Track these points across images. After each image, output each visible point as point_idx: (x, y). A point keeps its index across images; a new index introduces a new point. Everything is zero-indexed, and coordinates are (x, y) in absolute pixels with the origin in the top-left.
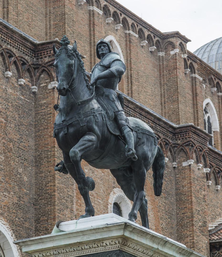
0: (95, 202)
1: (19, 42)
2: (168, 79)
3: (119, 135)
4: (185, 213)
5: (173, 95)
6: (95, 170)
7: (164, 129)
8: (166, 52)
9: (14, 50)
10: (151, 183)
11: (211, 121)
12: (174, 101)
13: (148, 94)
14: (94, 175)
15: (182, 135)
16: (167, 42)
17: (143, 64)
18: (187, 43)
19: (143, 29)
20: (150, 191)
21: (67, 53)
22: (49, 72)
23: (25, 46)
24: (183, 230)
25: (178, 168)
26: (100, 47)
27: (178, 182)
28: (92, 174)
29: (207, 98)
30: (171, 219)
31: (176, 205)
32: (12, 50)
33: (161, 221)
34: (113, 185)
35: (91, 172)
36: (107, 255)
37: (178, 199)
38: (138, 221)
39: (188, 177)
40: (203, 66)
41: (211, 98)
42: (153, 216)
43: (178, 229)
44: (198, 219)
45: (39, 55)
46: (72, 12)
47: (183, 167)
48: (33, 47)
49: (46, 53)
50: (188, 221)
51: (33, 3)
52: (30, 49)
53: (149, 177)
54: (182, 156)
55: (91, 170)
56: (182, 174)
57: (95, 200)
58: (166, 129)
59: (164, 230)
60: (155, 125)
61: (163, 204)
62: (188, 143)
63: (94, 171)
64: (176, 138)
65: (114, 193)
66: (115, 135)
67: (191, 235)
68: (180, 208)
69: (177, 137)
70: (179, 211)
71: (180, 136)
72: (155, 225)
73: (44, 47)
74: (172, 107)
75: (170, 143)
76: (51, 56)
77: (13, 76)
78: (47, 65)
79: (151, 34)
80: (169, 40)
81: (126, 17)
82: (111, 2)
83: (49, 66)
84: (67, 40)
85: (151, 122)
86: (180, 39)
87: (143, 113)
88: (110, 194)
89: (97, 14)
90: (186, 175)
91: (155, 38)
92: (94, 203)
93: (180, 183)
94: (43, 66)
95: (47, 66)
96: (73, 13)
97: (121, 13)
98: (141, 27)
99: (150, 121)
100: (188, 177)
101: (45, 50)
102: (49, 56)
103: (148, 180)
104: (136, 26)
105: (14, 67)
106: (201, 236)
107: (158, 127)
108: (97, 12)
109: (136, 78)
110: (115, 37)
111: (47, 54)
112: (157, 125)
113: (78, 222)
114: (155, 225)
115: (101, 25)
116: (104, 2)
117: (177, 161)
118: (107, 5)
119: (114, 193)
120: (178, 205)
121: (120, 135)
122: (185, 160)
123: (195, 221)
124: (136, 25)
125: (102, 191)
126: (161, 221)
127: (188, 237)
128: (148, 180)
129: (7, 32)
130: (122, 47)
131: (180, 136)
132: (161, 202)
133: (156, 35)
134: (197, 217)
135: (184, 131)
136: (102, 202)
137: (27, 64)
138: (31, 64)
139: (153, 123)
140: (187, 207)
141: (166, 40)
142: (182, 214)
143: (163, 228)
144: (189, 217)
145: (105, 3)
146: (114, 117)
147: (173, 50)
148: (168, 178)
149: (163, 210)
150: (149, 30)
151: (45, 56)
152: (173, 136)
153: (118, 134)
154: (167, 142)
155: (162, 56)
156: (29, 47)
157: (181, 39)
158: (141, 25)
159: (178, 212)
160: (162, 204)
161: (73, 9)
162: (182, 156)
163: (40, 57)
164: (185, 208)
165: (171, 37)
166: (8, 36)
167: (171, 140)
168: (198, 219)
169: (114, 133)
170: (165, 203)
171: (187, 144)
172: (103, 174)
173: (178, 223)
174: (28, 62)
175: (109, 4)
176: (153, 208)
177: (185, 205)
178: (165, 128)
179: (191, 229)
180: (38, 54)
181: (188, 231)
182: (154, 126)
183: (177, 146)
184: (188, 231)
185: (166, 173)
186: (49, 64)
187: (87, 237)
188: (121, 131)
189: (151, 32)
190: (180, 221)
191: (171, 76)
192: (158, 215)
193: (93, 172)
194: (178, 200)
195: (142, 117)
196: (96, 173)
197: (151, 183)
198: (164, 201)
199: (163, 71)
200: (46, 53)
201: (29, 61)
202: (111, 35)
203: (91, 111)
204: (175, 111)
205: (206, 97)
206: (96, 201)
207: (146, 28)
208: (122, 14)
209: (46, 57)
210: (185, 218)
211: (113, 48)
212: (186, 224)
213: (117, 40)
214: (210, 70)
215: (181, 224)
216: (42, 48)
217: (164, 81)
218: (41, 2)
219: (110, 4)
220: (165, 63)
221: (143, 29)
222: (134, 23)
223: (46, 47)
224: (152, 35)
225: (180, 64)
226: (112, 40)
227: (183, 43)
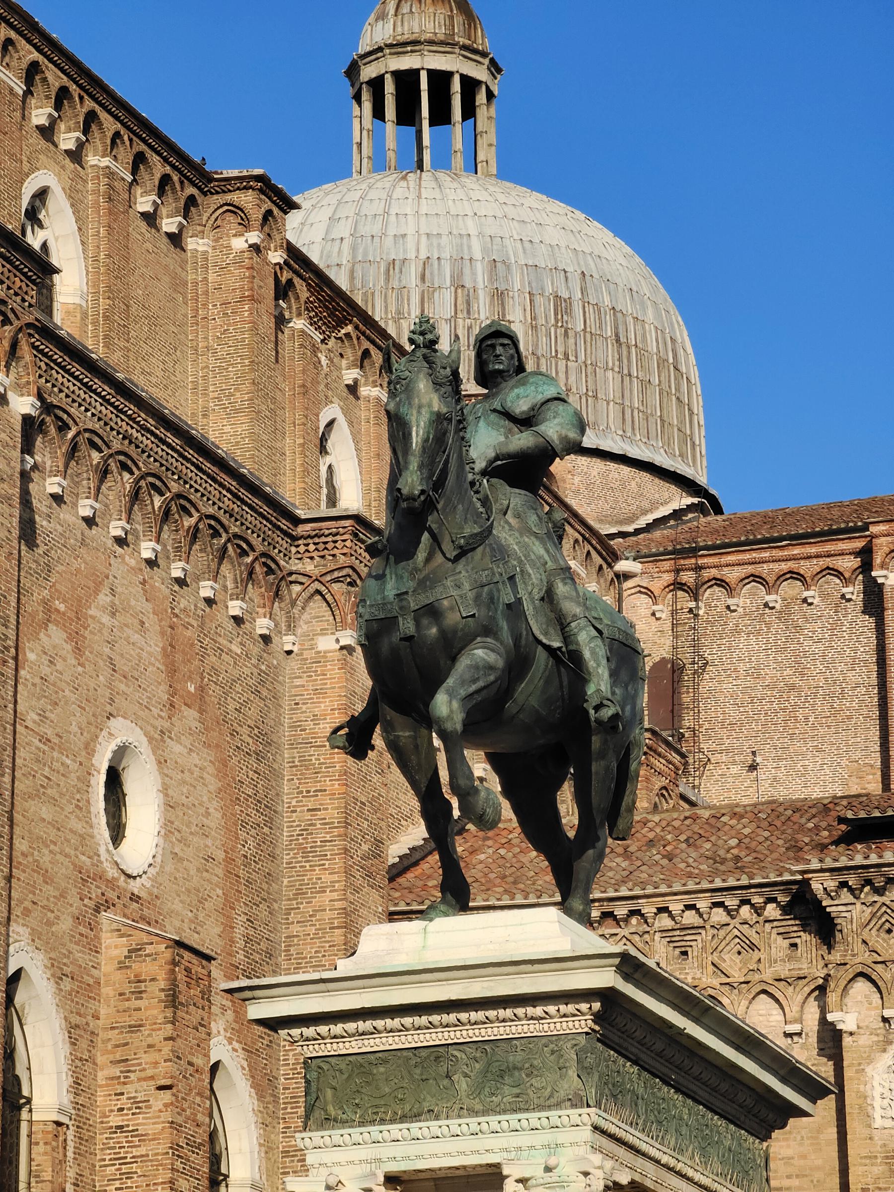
0: (54, 763)
2: (218, 334)
3: (559, 649)
4: (320, 810)
5: (235, 389)
6: (56, 655)
7: (265, 522)
8: (216, 241)
10: (220, 704)
11: (337, 482)
12: (237, 411)
13: (154, 380)
14: (55, 673)
15: (321, 546)
16: (221, 206)
17: (142, 275)
18: (286, 213)
19: (149, 154)
20: (214, 730)
24: (307, 864)
25: (302, 654)
26: (493, 346)
27: (297, 704)
28: (49, 666)
29: (332, 402)
30: (271, 828)
31: (288, 780)
33: (242, 835)
34: (108, 708)
35: (47, 662)
36: (545, 1049)
37: (297, 760)
38: (176, 833)
39: (334, 688)
40: (325, 292)
41: (342, 404)
42: (219, 815)
43: (291, 863)
44: (361, 830)
47: (320, 652)
50: (328, 839)
53: (216, 683)
54: (318, 617)
55: (45, 653)
56: (314, 678)
57: (53, 758)
58: (271, 522)
59: (251, 864)
60: (238, 506)
61: (250, 776)
62: (340, 575)
63: (54, 658)
64: (298, 552)
65: (110, 733)
66: (547, 648)
67: (337, 885)
68: (302, 792)
69: (302, 549)
70: (297, 802)
71: (312, 547)
72: (223, 845)
74: (227, 429)
75: (281, 570)
79: (171, 174)
80: (228, 197)
81: (98, 109)
84: (431, 332)
85: (229, 495)
86: (267, 200)
87: (207, 466)
88: (97, 737)
90: (328, 681)
91: (182, 189)
92: (50, 768)
93: (304, 707)
97: (82, 93)
98: (143, 147)
99: (224, 492)
100: (334, 688)
103: (211, 692)
104: (128, 143)
106: (367, 889)
107: (247, 513)
108: (9, 86)
109: (122, 323)
110: (58, 175)
112: (244, 507)
113: (429, 929)
114: (223, 845)
115: (17, 134)
116: (31, 53)
117: (299, 631)
118: (38, 62)
119: (110, 733)
120: (296, 781)
121: (564, 649)
122: (327, 629)
123: (352, 839)
124: (126, 138)
125: (74, 728)
126: (242, 835)
127: (325, 892)
128: (211, 692)
130: (79, 212)
131: (312, 547)
132: (244, 768)
133: (187, 178)
134: (358, 825)
135: (327, 532)
136: (73, 766)
139: (235, 500)
140: (325, 790)
141: (215, 197)
142: (309, 810)
143: (245, 856)
144: (333, 823)
145: (35, 56)
146: (545, 588)
147: (243, 235)
148: (268, 689)
149: (250, 797)
150: (166, 160)
152: (291, 545)
153: (556, 644)
154: (273, 566)
155: (205, 253)
157: (270, 198)
158: (144, 141)
159: (294, 803)
160: (248, 776)
162: (318, 617)
164: (320, 791)
165: (238, 189)
167: (285, 561)
168: (361, 830)
169: (544, 641)
170: (255, 772)
171: (336, 574)
172: (80, 669)
173: (291, 841)
176: (221, 790)
177: (320, 781)
178: (267, 520)
179: (336, 864)
181: (325, 869)
182: (236, 509)
183: (301, 579)
184: (325, 869)
185: (264, 673)
187: (485, 984)
188: (567, 638)
189: (173, 166)
190: (298, 835)
191: (228, 325)
192: (234, 812)
193: (50, 661)
194: (297, 763)
195: (201, 478)
196: (59, 667)
197: (220, 704)
198: (255, 765)
199: (205, 305)
202: (46, 168)
203: (492, 569)
204: (237, 443)
205: (328, 401)
206: (57, 761)
207: (159, 154)
208: (86, 97)
210: (319, 826)
211: (50, 213)
212: (321, 846)
213: (63, 189)
214: (345, 310)
215: (302, 844)
217: (206, 338)
219: (51, 60)
220: (210, 279)
221: (149, 154)
222: (122, 133)
224: (175, 178)
225: (262, 284)
226: (48, 187)
227: (276, 211)
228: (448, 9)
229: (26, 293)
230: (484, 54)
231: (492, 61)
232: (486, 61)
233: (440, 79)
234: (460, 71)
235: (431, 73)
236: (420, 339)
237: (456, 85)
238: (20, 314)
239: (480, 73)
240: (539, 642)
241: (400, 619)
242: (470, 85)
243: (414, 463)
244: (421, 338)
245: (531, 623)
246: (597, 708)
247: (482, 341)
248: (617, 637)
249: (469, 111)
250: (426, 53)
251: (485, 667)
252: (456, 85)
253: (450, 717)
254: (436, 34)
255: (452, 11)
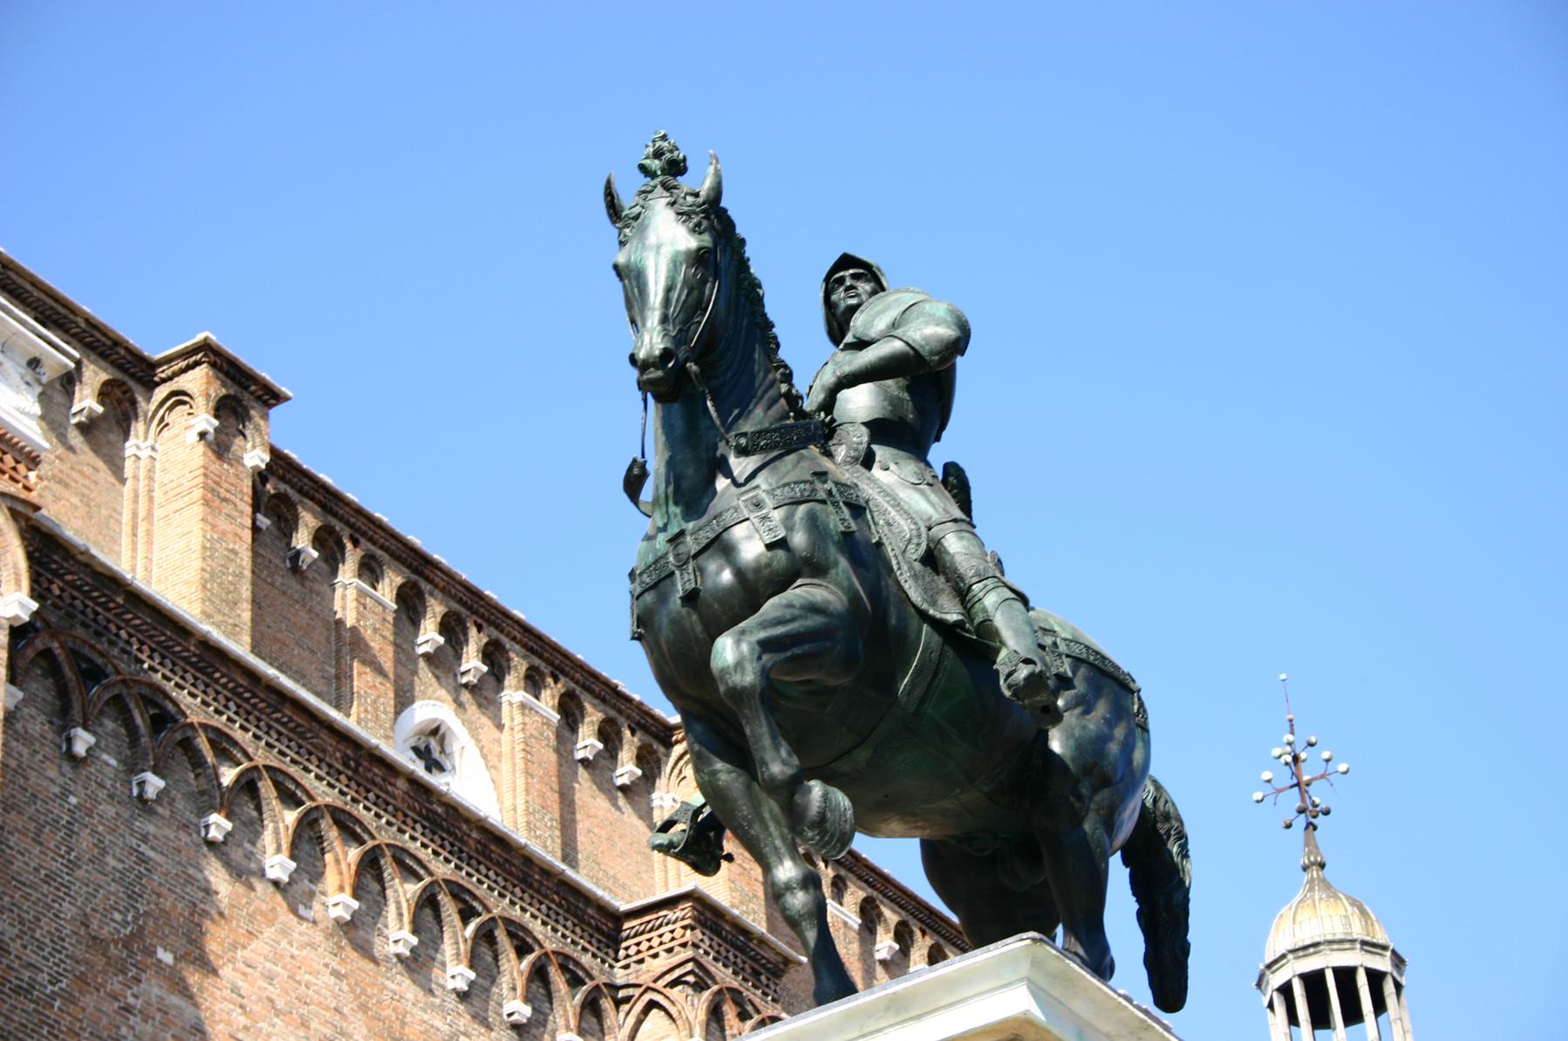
1: (553, 901)
9: (537, 927)
21: (672, 204)
22: (673, 1010)
23: (575, 916)
26: (841, 281)
32: (530, 926)
45: (633, 950)
46: (751, 905)
48: (610, 924)
49: (655, 942)
51: (614, 877)
52: (598, 929)
66: (938, 625)
73: (649, 922)
76: (677, 949)
77: (536, 1020)
78: (660, 985)
82: (886, 888)
83: (672, 987)
89: (841, 925)
94: (648, 989)
95: (665, 986)
96: (756, 908)
101: (651, 930)
102: (670, 950)
105: (541, 990)
111: (661, 943)
118: (872, 897)
129: (506, 860)
137: (587, 980)
138: (605, 984)
151: (652, 952)
156: (593, 922)
161: (755, 896)
163: (635, 958)
166: (511, 874)
174: (592, 978)
175: (880, 897)
180: (627, 948)
186: (668, 978)
200: (655, 942)
201: (595, 973)
209: (655, 956)
216: (641, 924)
218: (643, 876)
223: (658, 919)
228: (1342, 908)
229: (767, 986)
230: (1384, 948)
231: (1394, 952)
232: (1388, 954)
233: (1345, 976)
234: (1365, 964)
235: (1337, 971)
236: (655, 164)
237: (1362, 980)
238: (760, 1007)
239: (1383, 964)
240: (924, 616)
241: (677, 573)
242: (1376, 978)
243: (653, 318)
244: (657, 162)
245: (906, 586)
246: (1010, 674)
247: (827, 279)
248: (1084, 656)
249: (1380, 1006)
250: (1328, 952)
251: (803, 608)
252: (1362, 980)
253: (739, 665)
254: (1334, 934)
255: (1346, 911)
